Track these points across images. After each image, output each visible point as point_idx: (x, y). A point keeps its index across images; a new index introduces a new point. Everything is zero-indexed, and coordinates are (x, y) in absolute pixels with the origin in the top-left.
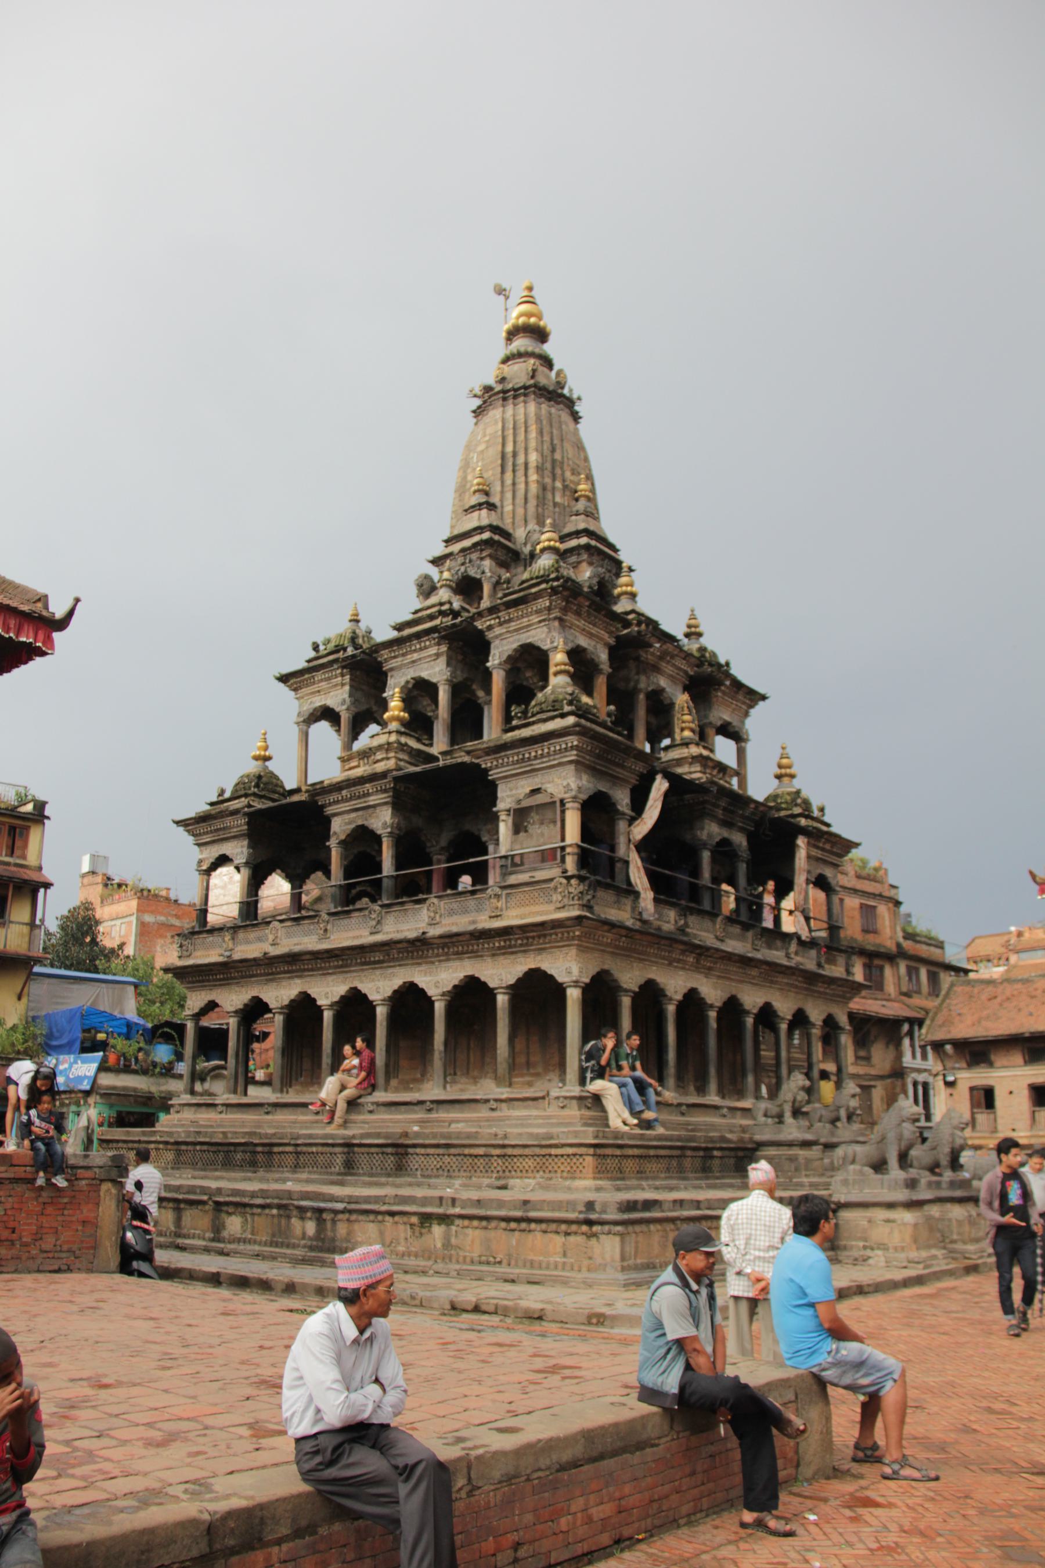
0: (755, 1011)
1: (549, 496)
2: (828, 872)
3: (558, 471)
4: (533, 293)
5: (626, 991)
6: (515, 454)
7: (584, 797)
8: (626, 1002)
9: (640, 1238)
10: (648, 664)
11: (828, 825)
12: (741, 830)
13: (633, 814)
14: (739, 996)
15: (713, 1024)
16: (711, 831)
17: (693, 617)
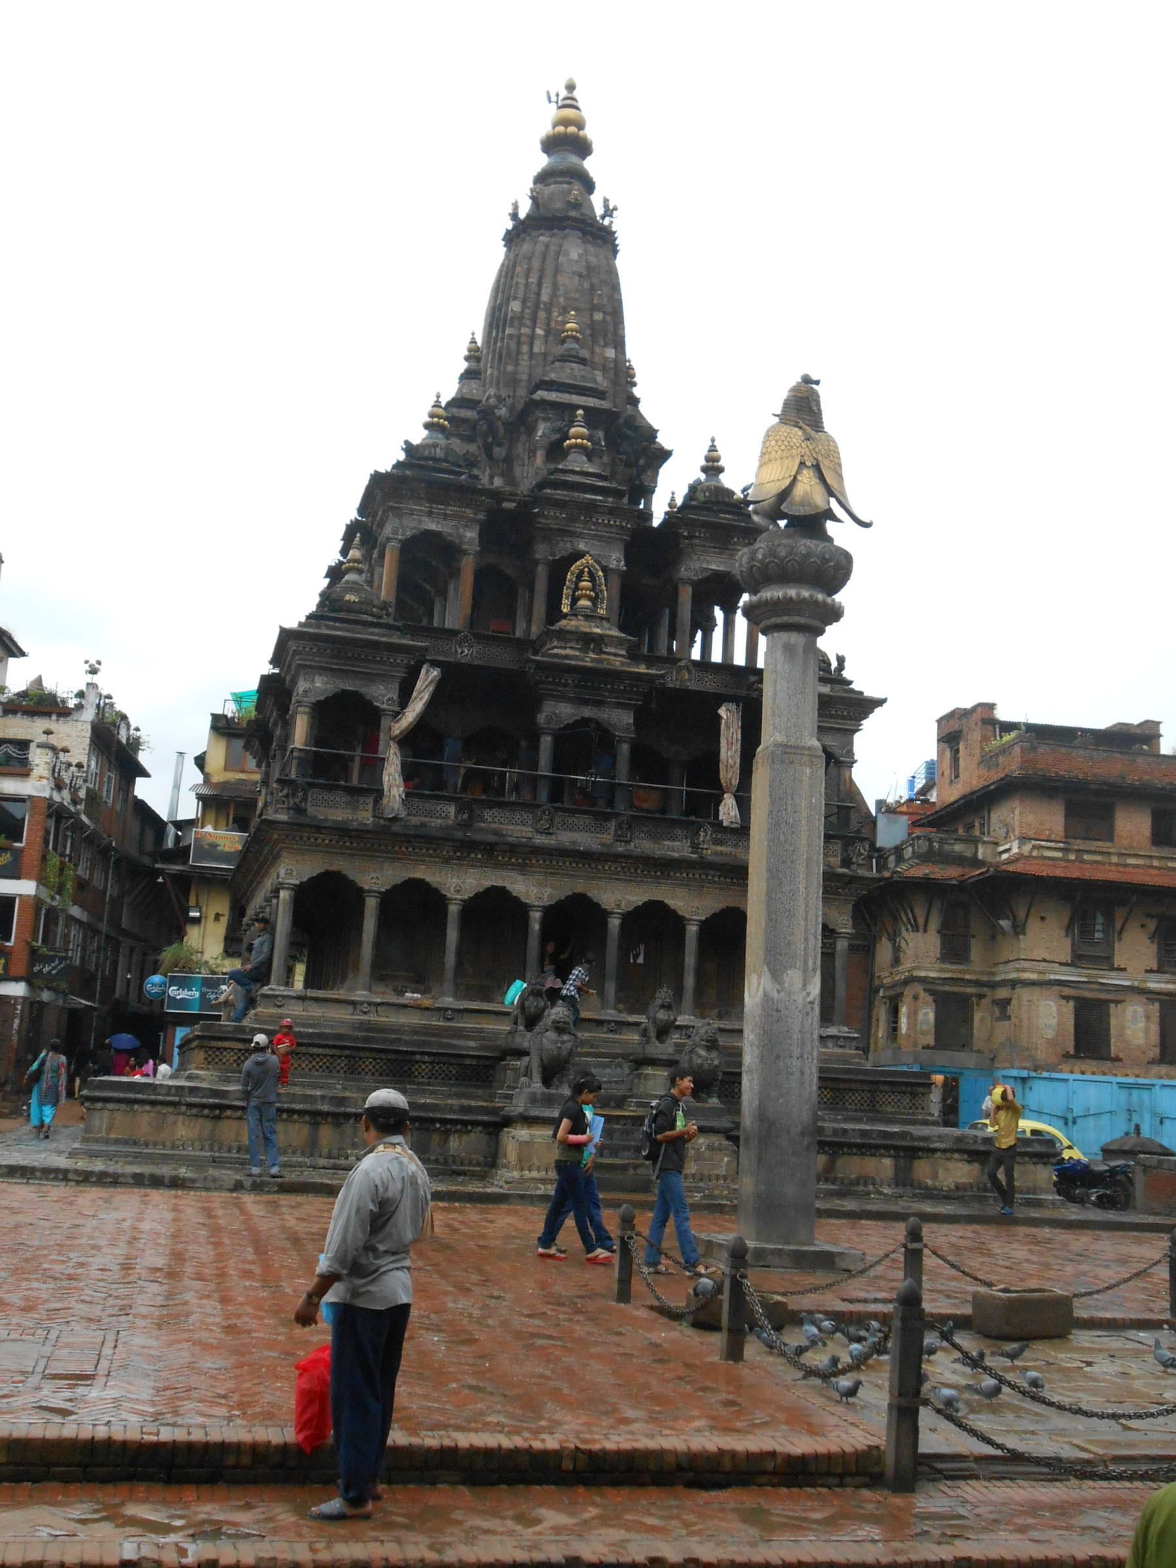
0: (626, 907)
1: (525, 348)
3: (542, 315)
4: (576, 94)
5: (369, 891)
7: (313, 700)
8: (371, 904)
9: (118, 1116)
10: (551, 529)
11: (851, 682)
12: (619, 705)
13: (397, 709)
14: (589, 894)
15: (537, 927)
16: (558, 712)
17: (713, 449)
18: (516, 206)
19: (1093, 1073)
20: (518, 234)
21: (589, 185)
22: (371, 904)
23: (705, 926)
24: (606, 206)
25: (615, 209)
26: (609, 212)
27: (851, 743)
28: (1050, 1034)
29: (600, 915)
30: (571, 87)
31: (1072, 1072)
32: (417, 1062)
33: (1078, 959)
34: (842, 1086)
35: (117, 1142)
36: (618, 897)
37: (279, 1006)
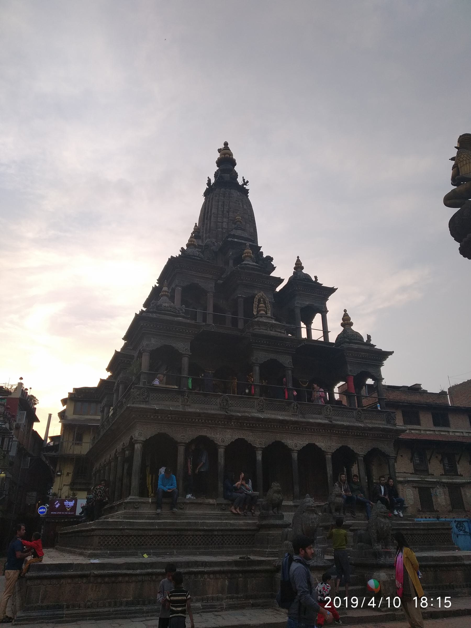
0: (299, 448)
2: (370, 370)
6: (208, 212)
8: (181, 449)
14: (283, 441)
18: (209, 180)
19: (430, 518)
20: (209, 192)
21: (236, 175)
22: (181, 449)
23: (333, 455)
24: (244, 180)
25: (248, 182)
26: (246, 183)
27: (379, 371)
28: (411, 502)
29: (287, 451)
30: (226, 144)
31: (422, 518)
32: (215, 535)
33: (417, 471)
34: (415, 532)
35: (48, 607)
36: (295, 443)
37: (136, 508)
